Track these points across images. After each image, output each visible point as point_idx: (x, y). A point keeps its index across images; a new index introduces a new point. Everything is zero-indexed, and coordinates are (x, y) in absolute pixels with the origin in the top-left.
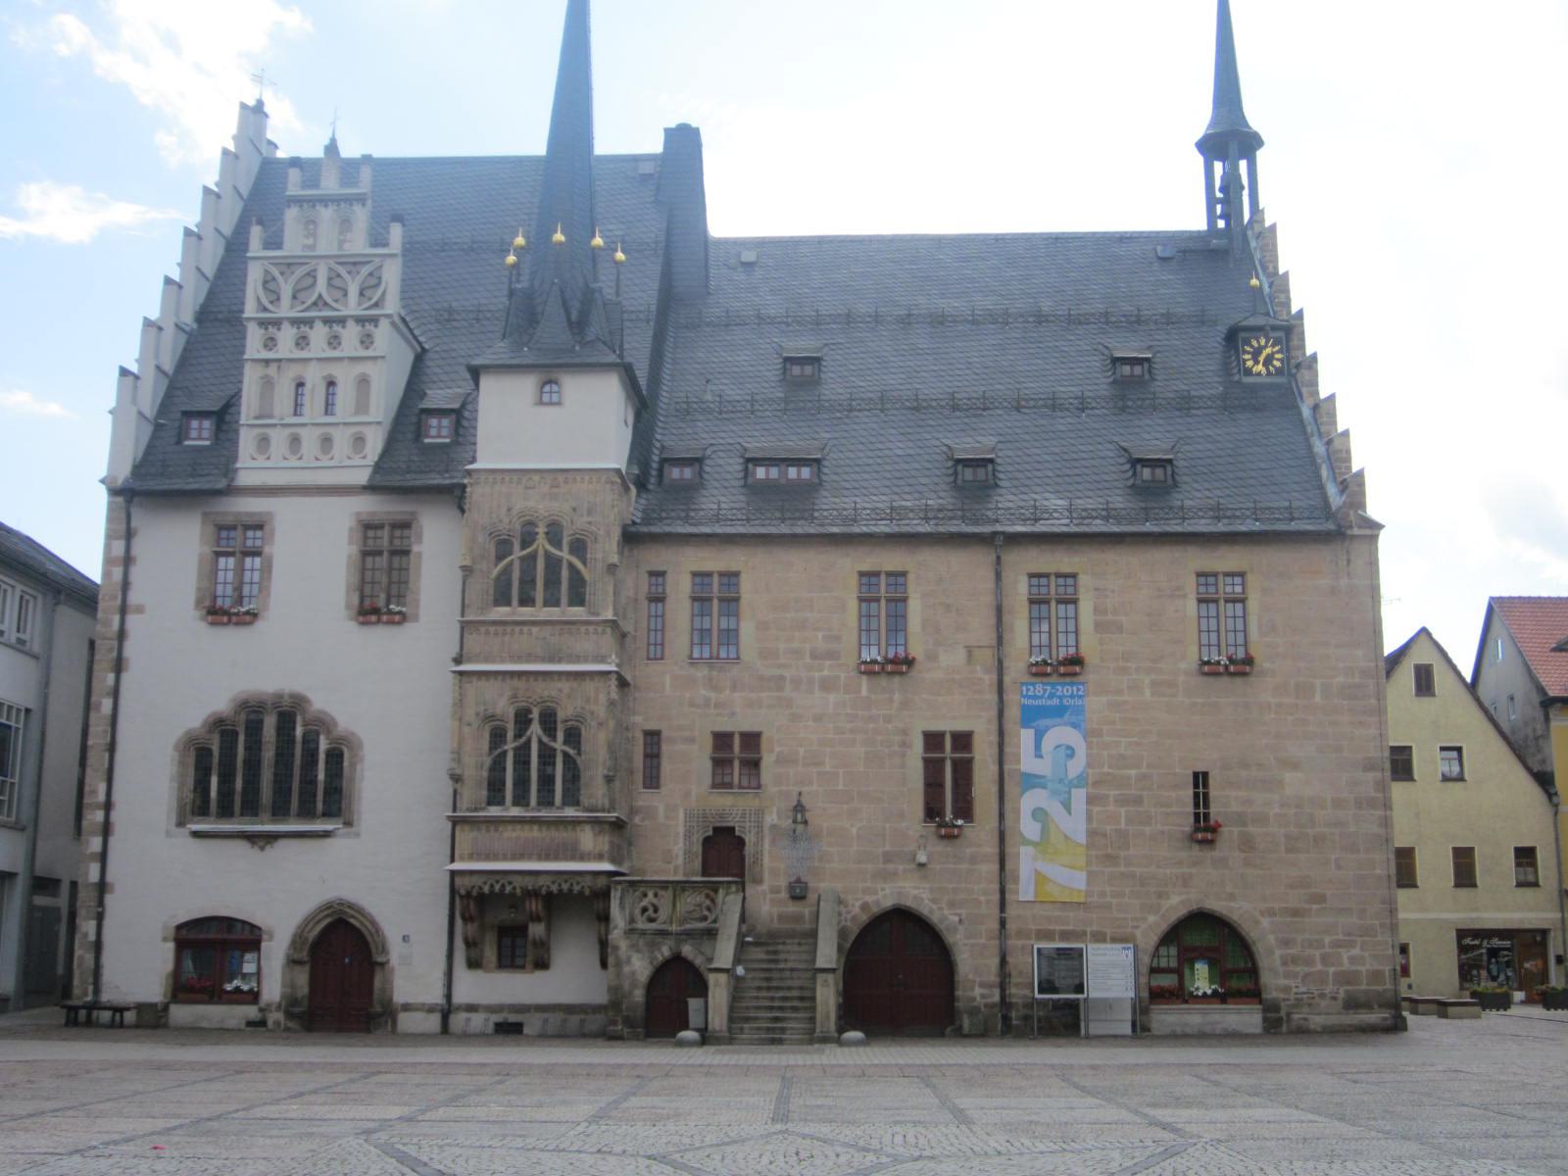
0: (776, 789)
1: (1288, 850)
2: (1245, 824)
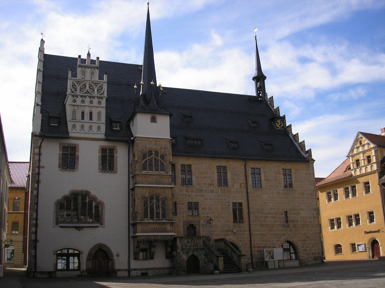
0: (202, 216)
1: (302, 228)
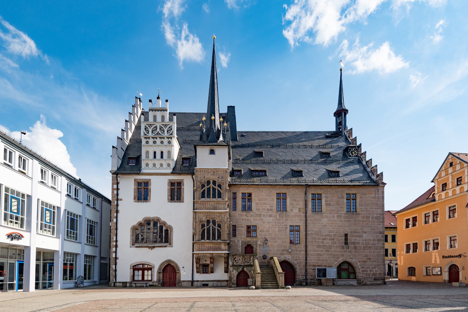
2: (355, 244)
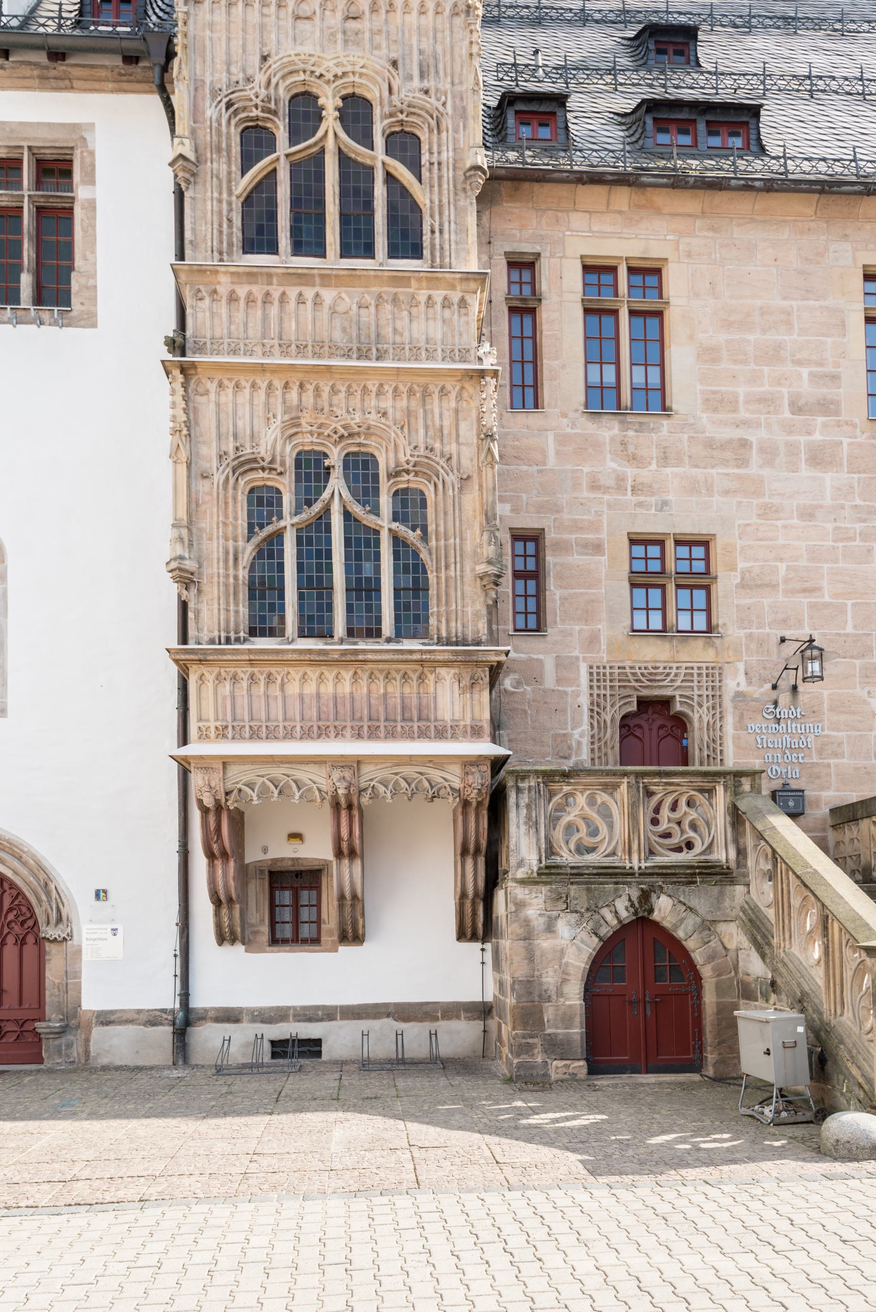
0: (742, 633)
